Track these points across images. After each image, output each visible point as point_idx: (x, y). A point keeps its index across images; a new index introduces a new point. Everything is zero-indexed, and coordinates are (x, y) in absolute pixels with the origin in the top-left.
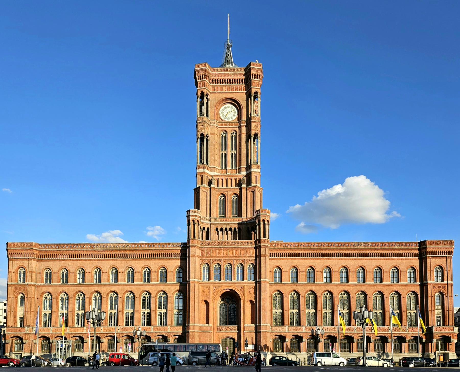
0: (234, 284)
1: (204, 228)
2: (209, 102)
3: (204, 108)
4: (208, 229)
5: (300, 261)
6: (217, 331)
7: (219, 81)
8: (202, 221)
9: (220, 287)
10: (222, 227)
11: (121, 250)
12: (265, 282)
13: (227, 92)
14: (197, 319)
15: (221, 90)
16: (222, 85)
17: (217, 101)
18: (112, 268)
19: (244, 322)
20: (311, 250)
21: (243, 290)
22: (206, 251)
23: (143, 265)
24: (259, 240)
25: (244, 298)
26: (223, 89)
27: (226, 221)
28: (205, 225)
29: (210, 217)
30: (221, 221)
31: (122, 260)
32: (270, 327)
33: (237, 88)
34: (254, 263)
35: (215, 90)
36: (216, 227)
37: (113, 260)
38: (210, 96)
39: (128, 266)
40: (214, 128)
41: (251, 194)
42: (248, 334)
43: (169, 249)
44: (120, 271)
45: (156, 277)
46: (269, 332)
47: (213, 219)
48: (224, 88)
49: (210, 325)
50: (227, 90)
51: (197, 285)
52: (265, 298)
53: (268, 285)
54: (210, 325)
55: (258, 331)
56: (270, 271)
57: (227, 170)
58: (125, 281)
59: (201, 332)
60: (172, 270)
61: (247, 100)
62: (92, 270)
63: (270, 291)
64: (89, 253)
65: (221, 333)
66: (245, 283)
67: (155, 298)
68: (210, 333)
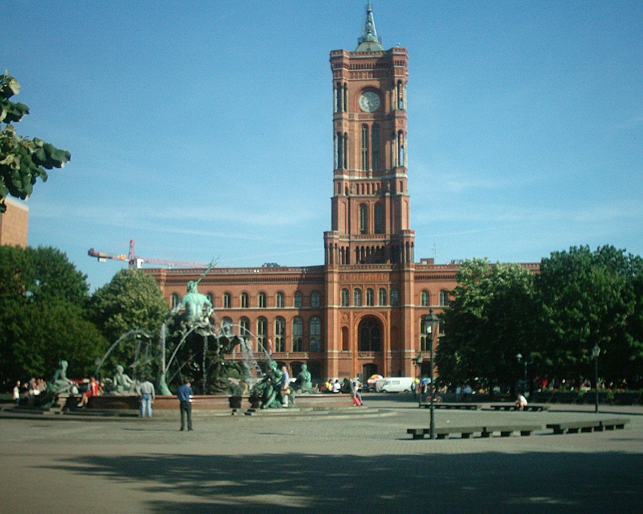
1: (343, 247)
2: (347, 92)
4: (347, 248)
7: (358, 67)
8: (340, 239)
12: (409, 307)
14: (335, 346)
15: (361, 77)
21: (386, 315)
27: (368, 238)
29: (349, 233)
36: (356, 245)
48: (363, 74)
49: (350, 352)
51: (335, 311)
53: (412, 311)
59: (341, 359)
60: (308, 295)
63: (415, 316)
66: (387, 308)
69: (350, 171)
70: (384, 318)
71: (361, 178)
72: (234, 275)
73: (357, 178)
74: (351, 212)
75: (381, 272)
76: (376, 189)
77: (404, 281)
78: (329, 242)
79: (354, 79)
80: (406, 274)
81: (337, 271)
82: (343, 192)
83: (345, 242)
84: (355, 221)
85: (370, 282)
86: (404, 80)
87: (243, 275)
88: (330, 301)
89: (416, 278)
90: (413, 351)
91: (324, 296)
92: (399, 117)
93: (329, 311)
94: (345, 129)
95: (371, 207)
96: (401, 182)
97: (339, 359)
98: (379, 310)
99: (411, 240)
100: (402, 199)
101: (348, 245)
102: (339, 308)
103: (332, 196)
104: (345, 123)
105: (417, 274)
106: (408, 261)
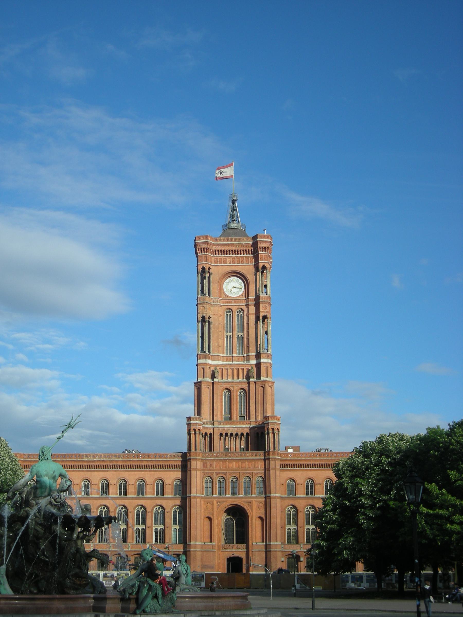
2: (211, 276)
3: (206, 281)
4: (211, 434)
6: (222, 550)
10: (227, 432)
11: (113, 461)
12: (275, 497)
13: (231, 264)
14: (199, 537)
15: (225, 262)
16: (226, 257)
17: (220, 275)
18: (102, 480)
19: (252, 540)
20: (329, 460)
21: (251, 505)
22: (208, 463)
23: (137, 477)
24: (269, 452)
25: (252, 514)
26: (227, 261)
27: (231, 424)
29: (213, 420)
30: (226, 424)
31: (114, 471)
32: (283, 546)
33: (242, 259)
34: (263, 476)
35: (218, 263)
36: (220, 432)
37: (103, 471)
39: (120, 478)
41: (260, 390)
42: (257, 553)
43: (167, 459)
44: (111, 483)
45: (152, 490)
46: (279, 551)
47: (216, 423)
48: (228, 260)
49: (214, 543)
50: (232, 261)
51: (198, 500)
53: (278, 500)
54: (214, 543)
55: (268, 550)
56: (282, 483)
57: (232, 357)
58: (117, 494)
60: (170, 483)
61: (256, 274)
62: (80, 482)
64: (77, 464)
66: (253, 498)
67: (151, 513)
69: (213, 356)
71: (225, 363)
72: (93, 461)
73: (221, 363)
74: (215, 397)
76: (241, 375)
78: (192, 427)
79: (218, 265)
80: (272, 462)
81: (200, 458)
83: (209, 429)
84: (219, 407)
85: (233, 470)
86: (267, 265)
87: (103, 461)
88: (193, 490)
89: (282, 466)
92: (263, 302)
93: (192, 500)
95: (235, 392)
96: (267, 367)
97: (202, 551)
98: (244, 500)
99: (276, 427)
100: (267, 384)
101: (212, 432)
102: (202, 498)
103: (196, 381)
104: (209, 307)
105: (284, 463)
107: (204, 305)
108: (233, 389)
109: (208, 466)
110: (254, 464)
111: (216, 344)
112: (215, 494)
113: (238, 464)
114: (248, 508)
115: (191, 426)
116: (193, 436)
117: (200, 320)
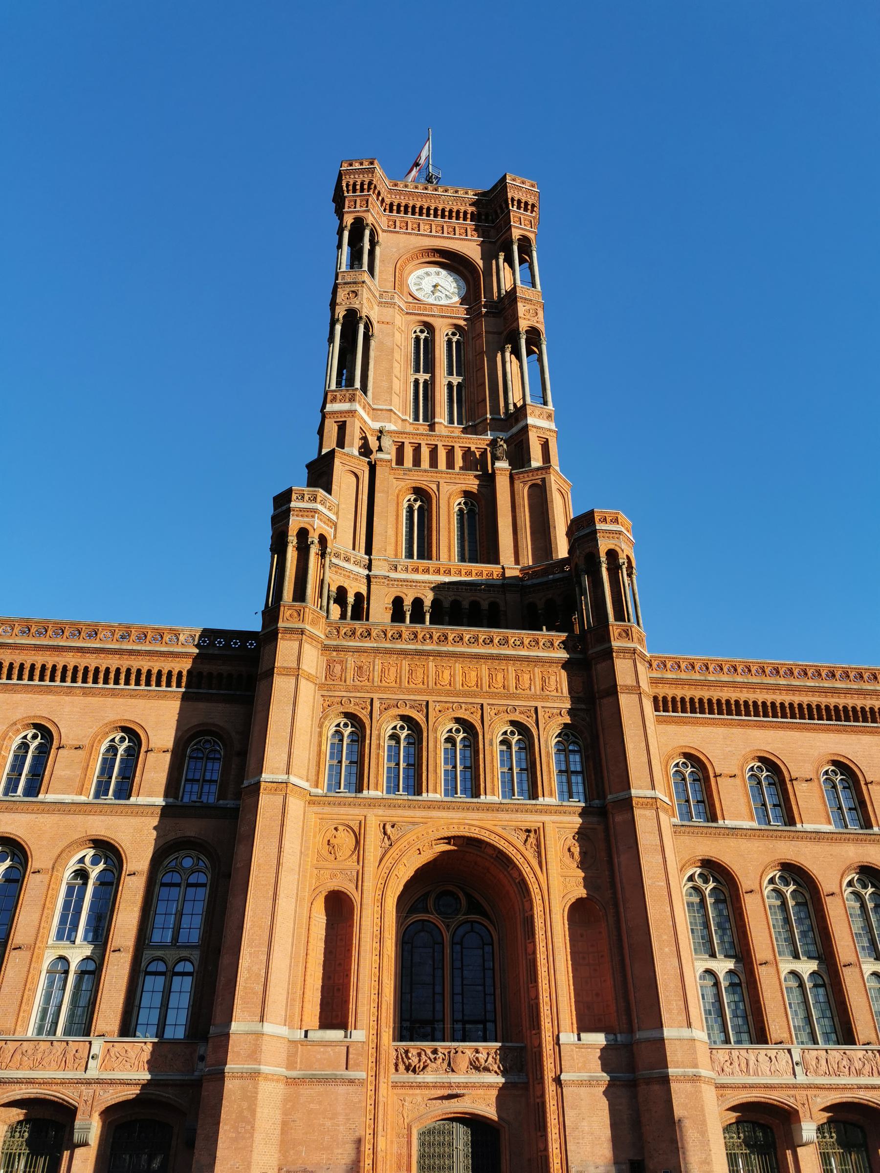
0: (489, 815)
2: (378, 250)
4: (358, 596)
5: (781, 733)
9: (414, 823)
10: (419, 595)
21: (538, 846)
23: (19, 714)
28: (347, 581)
29: (369, 551)
36: (393, 593)
38: (382, 237)
40: (391, 310)
42: (583, 1091)
45: (79, 772)
49: (358, 1035)
52: (663, 884)
65: (420, 1086)
68: (351, 1089)
70: (530, 855)
75: (507, 658)
77: (612, 691)
78: (295, 523)
82: (352, 445)
84: (391, 532)
90: (700, 1034)
91: (243, 754)
94: (369, 308)
106: (620, 615)
107: (353, 289)
108: (438, 490)
109: (350, 675)
110: (543, 680)
111: (385, 384)
112: (372, 785)
113: (474, 674)
114: (526, 853)
115: (292, 519)
116: (292, 554)
117: (341, 317)
